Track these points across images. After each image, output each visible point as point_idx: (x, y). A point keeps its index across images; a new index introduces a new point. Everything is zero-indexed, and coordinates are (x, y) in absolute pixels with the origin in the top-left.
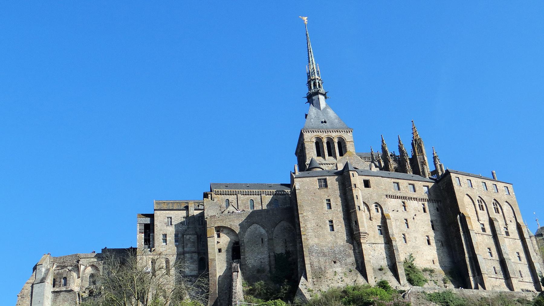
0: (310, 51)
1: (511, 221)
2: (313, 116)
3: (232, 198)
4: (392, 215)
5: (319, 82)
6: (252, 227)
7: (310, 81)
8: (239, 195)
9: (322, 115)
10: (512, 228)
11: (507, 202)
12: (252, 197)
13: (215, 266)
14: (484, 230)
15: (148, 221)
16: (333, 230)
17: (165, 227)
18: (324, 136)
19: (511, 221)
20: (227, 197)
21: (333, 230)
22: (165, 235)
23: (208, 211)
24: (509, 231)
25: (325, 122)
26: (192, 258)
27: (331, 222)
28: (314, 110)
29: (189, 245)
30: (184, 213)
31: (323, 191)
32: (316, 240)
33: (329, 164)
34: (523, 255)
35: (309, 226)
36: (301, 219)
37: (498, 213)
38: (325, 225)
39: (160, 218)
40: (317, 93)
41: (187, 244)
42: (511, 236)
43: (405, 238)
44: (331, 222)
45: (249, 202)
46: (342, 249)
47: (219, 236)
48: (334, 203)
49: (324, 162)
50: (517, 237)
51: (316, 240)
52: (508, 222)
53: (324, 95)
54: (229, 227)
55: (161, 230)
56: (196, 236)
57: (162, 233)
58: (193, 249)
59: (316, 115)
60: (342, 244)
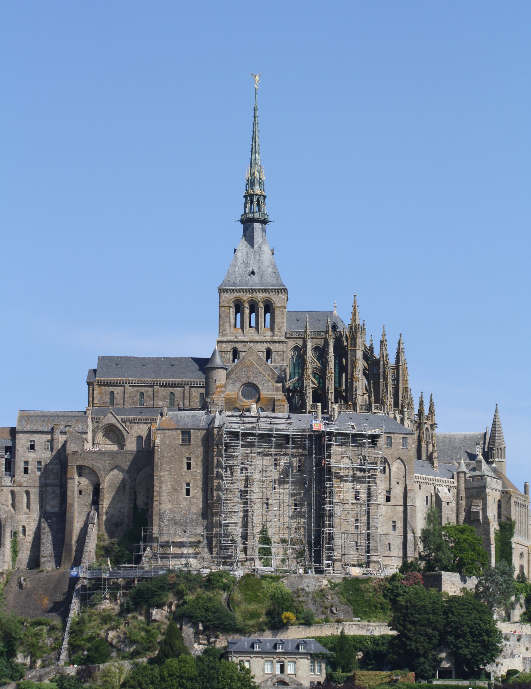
0: (255, 142)
1: (398, 483)
2: (240, 261)
3: (117, 390)
4: (256, 476)
5: (258, 199)
6: (115, 470)
7: (249, 198)
8: (127, 387)
9: (252, 257)
10: (398, 491)
11: (399, 458)
12: (142, 389)
13: (72, 513)
14: (356, 498)
15: (10, 444)
16: (188, 493)
17: (27, 453)
18: (246, 297)
19: (398, 483)
20: (112, 389)
21: (188, 493)
22: (26, 463)
23: (70, 445)
24: (392, 495)
25: (253, 273)
26: (53, 492)
27: (188, 484)
28: (244, 247)
29: (52, 477)
30: (49, 437)
31: (184, 449)
32: (169, 506)
33: (247, 342)
34: (400, 525)
35: (164, 488)
36: (156, 482)
37: (384, 473)
38: (182, 488)
39: (22, 441)
40: (253, 220)
41: (49, 476)
42: (392, 501)
43: (267, 504)
44: (188, 484)
45: (138, 396)
46: (195, 517)
47: (80, 475)
48: (194, 463)
49: (241, 338)
50: (401, 502)
51: (169, 506)
52: (393, 484)
53: (264, 222)
54: (91, 467)
55: (23, 456)
56: (59, 466)
57: (23, 459)
58: (56, 482)
59: (245, 256)
60: (195, 511)
